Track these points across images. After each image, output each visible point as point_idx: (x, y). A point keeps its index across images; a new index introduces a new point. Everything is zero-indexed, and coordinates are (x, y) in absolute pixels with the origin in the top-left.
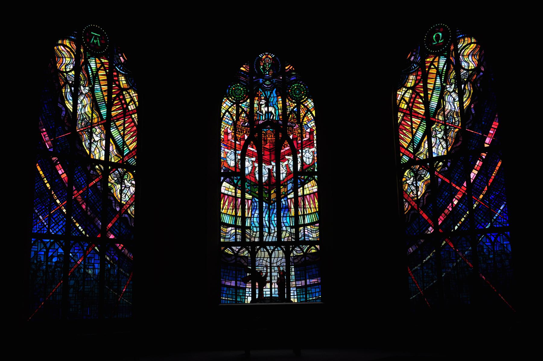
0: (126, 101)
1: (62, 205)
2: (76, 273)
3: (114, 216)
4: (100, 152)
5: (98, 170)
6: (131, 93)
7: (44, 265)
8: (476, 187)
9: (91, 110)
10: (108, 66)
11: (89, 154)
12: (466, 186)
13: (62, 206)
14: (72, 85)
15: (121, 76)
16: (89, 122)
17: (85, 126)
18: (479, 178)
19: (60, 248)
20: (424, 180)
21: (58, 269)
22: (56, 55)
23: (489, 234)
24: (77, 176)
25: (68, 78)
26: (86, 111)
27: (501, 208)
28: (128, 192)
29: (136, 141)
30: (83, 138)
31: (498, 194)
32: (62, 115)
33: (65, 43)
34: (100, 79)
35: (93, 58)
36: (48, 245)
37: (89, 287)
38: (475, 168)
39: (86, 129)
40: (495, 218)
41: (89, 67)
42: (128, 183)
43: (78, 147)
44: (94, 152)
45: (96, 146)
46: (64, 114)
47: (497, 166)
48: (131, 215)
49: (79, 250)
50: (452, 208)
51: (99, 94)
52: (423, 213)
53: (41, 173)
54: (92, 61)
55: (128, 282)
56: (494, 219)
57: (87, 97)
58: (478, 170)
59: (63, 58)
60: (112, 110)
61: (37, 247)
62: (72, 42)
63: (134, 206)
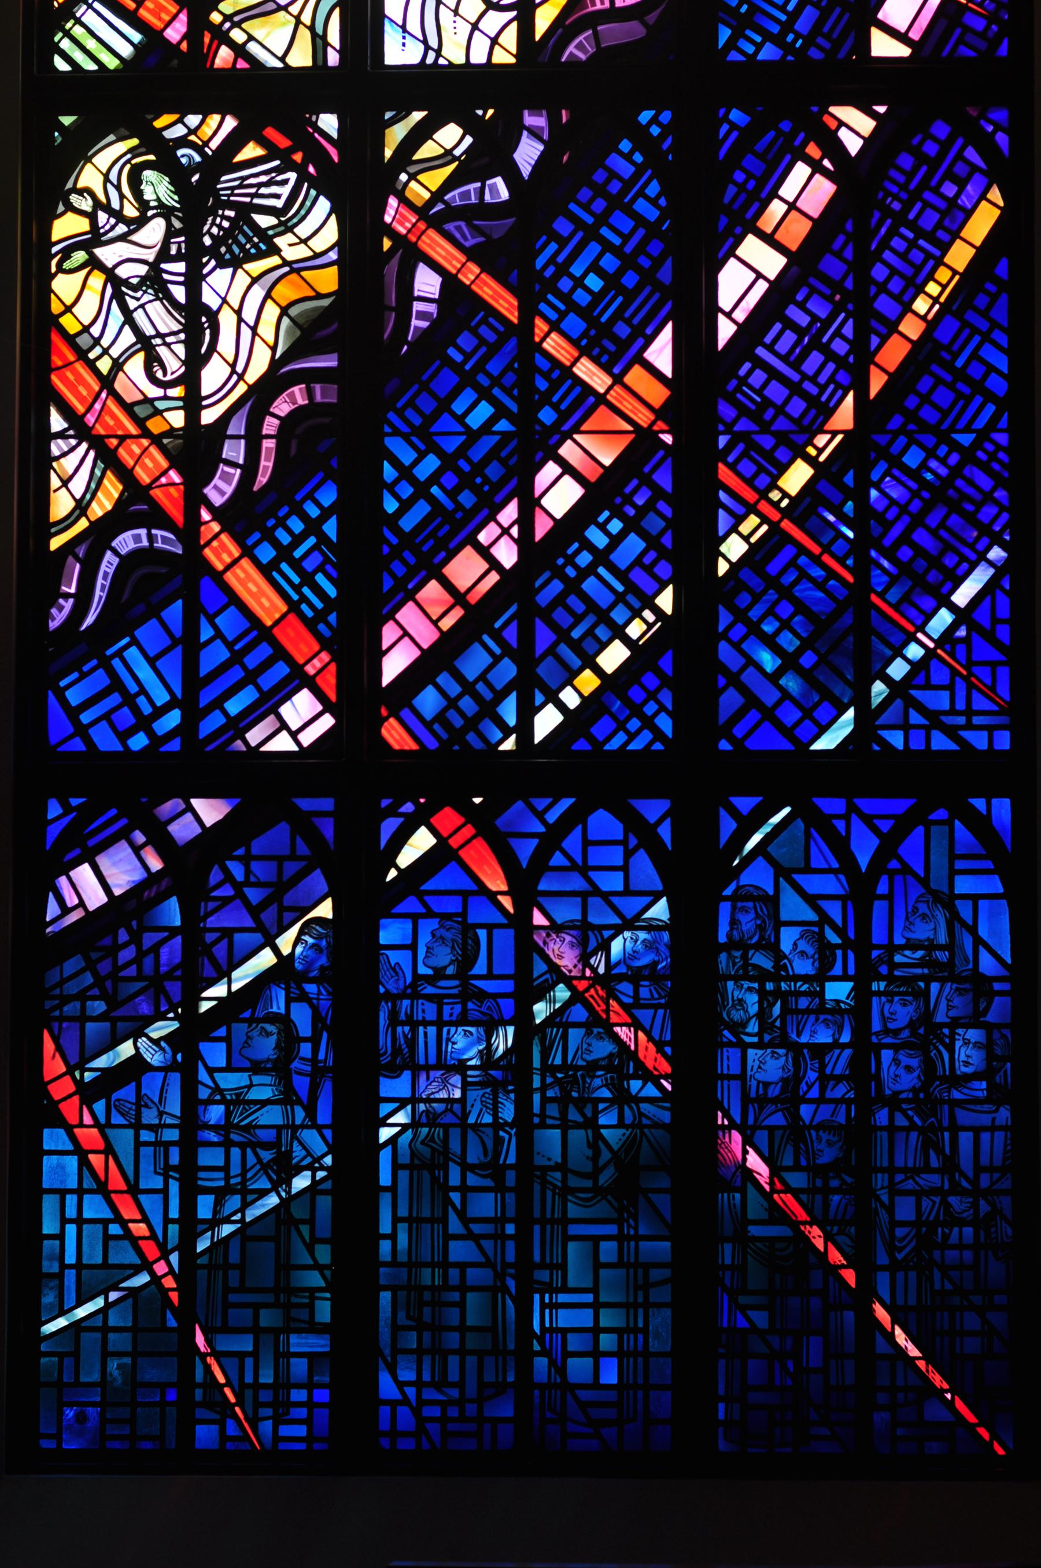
8: (759, 392)
12: (667, 370)
18: (794, 313)
20: (274, 261)
23: (831, 805)
27: (962, 597)
31: (943, 471)
38: (769, 230)
40: (898, 670)
47: (955, 234)
50: (525, 542)
52: (235, 562)
56: (888, 680)
58: (794, 247)
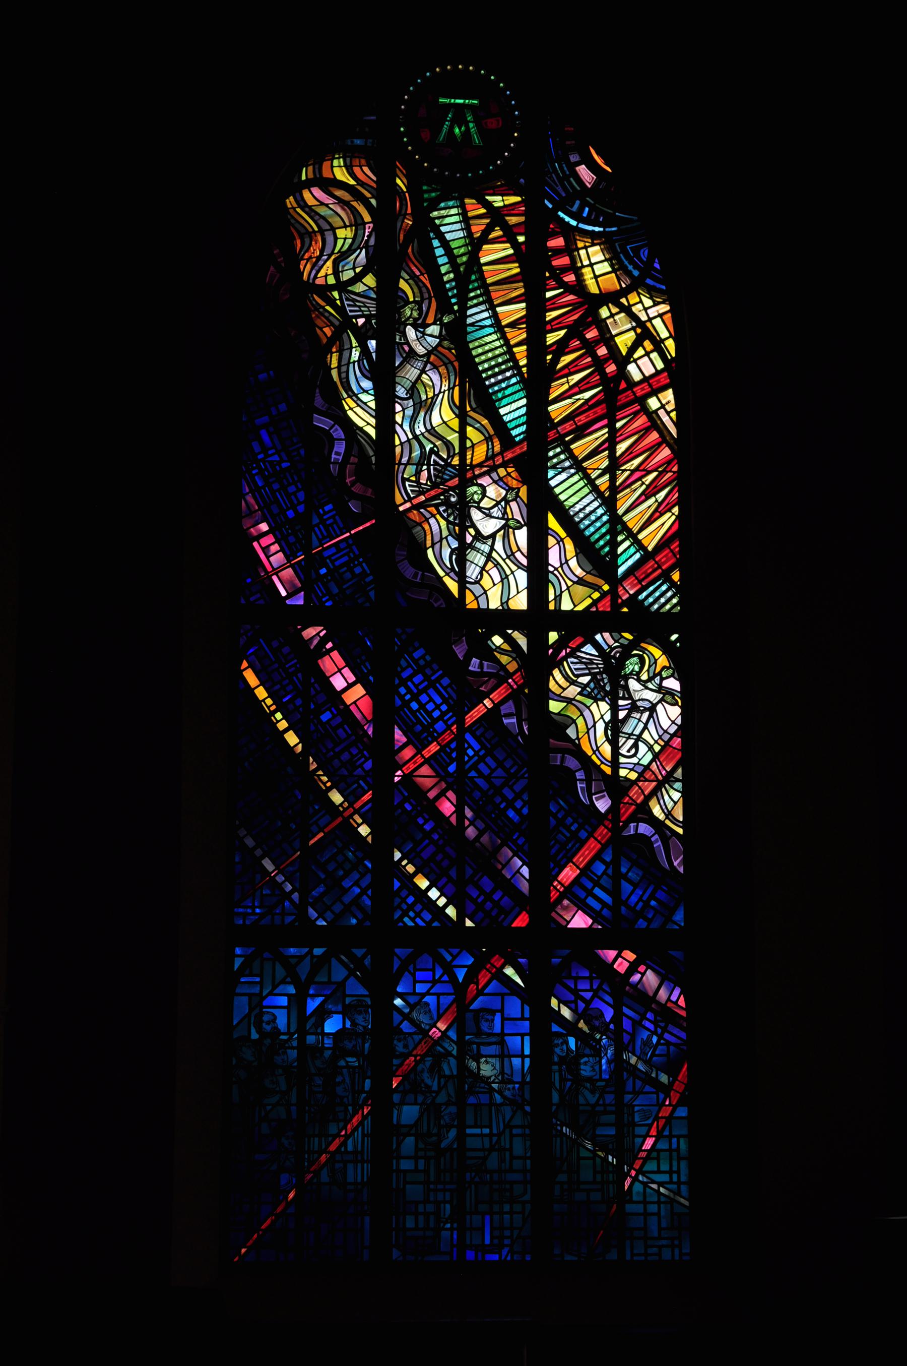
0: (613, 349)
1: (351, 810)
2: (426, 1075)
3: (583, 834)
4: (504, 578)
5: (504, 652)
6: (640, 306)
7: (293, 1048)
9: (457, 416)
10: (522, 219)
11: (456, 595)
13: (354, 814)
14: (367, 331)
15: (586, 248)
16: (450, 465)
17: (435, 485)
19: (352, 980)
21: (349, 1059)
22: (295, 228)
24: (409, 691)
25: (348, 309)
26: (436, 420)
28: (645, 727)
29: (673, 506)
30: (428, 532)
32: (333, 456)
33: (326, 174)
34: (489, 281)
35: (451, 203)
36: (304, 970)
37: (486, 1131)
39: (436, 497)
41: (436, 243)
42: (647, 688)
43: (409, 571)
44: (477, 582)
45: (489, 557)
46: (342, 450)
48: (668, 822)
49: (434, 982)
51: (487, 344)
53: (261, 693)
54: (447, 216)
55: (665, 1112)
57: (435, 367)
59: (322, 231)
60: (551, 397)
61: (258, 979)
62: (356, 162)
63: (678, 785)
